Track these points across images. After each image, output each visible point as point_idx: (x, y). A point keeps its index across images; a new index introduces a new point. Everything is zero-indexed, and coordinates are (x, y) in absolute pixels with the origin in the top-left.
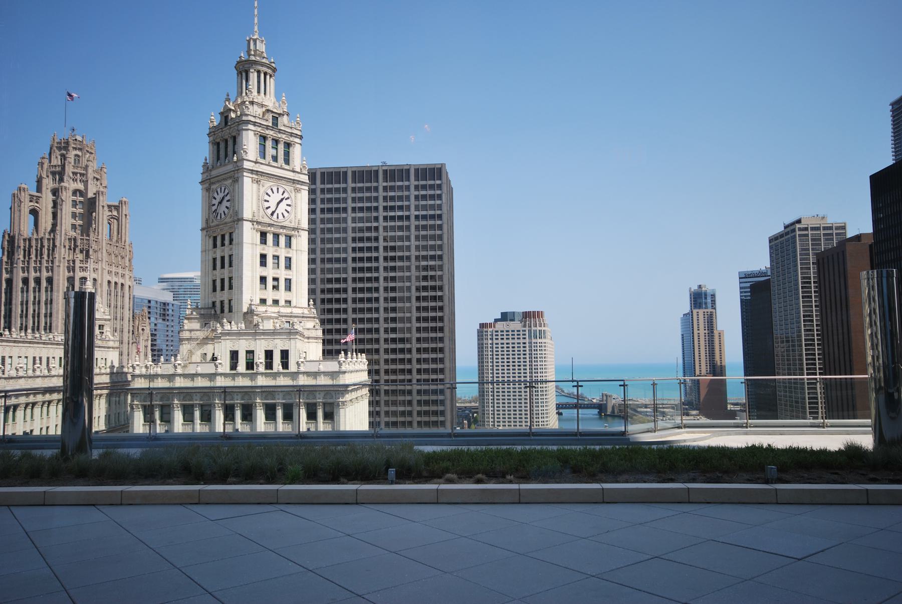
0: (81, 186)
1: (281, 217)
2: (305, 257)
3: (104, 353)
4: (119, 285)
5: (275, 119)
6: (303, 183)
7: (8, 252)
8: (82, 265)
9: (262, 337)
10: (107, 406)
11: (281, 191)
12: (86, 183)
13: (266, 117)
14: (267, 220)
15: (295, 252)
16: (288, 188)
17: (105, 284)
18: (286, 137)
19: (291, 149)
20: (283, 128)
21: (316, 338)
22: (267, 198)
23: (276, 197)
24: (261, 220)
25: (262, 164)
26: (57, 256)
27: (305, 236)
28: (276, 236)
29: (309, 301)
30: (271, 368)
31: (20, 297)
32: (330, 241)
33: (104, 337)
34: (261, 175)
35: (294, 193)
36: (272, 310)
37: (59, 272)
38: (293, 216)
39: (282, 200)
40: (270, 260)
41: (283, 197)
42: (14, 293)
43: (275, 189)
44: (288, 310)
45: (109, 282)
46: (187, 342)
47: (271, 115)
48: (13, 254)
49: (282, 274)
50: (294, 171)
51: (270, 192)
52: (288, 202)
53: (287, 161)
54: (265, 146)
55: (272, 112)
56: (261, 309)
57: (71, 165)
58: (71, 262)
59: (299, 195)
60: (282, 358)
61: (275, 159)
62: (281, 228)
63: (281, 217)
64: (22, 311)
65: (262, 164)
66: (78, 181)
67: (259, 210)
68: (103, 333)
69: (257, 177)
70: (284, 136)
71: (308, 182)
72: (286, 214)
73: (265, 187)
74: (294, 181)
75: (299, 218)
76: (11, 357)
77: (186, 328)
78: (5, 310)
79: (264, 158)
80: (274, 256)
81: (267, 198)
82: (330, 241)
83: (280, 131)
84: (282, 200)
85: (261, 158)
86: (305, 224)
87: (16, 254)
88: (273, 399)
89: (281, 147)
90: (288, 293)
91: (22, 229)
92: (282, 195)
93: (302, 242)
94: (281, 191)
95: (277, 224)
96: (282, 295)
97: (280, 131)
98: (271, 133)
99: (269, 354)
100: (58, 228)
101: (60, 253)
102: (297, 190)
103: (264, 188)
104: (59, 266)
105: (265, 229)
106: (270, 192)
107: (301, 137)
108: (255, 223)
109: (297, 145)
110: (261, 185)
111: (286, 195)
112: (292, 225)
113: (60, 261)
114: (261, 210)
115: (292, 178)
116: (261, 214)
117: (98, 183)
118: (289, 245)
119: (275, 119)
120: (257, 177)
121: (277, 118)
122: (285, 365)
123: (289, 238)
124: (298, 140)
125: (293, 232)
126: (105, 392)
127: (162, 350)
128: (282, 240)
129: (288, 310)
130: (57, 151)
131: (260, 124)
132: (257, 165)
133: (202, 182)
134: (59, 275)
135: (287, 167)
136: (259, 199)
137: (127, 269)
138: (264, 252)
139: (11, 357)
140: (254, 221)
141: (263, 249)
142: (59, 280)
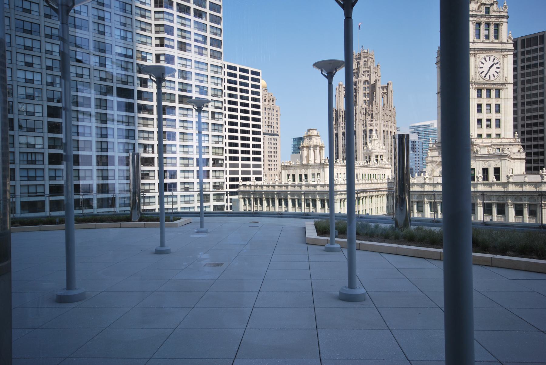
0: (367, 78)
1: (492, 77)
2: (511, 102)
3: (374, 171)
4: (386, 132)
5: (487, 9)
6: (509, 50)
7: (336, 119)
8: (370, 123)
9: (480, 159)
10: (387, 200)
11: (492, 58)
12: (370, 76)
13: (480, 9)
14: (482, 81)
15: (503, 100)
16: (497, 56)
17: (382, 132)
18: (496, 20)
19: (500, 27)
20: (493, 14)
21: (521, 159)
22: (481, 65)
23: (489, 63)
24: (477, 81)
25: (477, 43)
26: (357, 119)
27: (511, 88)
28: (489, 91)
29: (514, 133)
30: (487, 180)
31: (342, 143)
32: (529, 89)
33: (383, 162)
34: (477, 51)
35: (502, 58)
36: (487, 141)
37: (359, 128)
38: (501, 75)
39: (493, 65)
40: (484, 108)
41: (493, 63)
42: (339, 141)
43: (487, 59)
44: (498, 141)
45: (384, 131)
46: (430, 164)
47: (484, 6)
48: (338, 120)
49: (494, 116)
50: (502, 43)
51: (484, 61)
52: (498, 65)
53: (496, 37)
54: (479, 30)
55: (485, 4)
56: (479, 141)
57: (362, 67)
58: (364, 121)
59: (506, 59)
60: (495, 173)
61: (487, 37)
62: (492, 85)
63: (492, 77)
64: (343, 150)
65: (477, 43)
66: (366, 75)
67: (476, 75)
68: (382, 160)
69: (474, 53)
70: (494, 19)
71: (513, 48)
72: (496, 74)
73: (480, 58)
74: (502, 50)
75: (506, 75)
76: (341, 174)
77: (429, 155)
78: (336, 149)
79: (479, 38)
80: (487, 105)
81: (481, 65)
82: (529, 89)
83: (491, 17)
84: (493, 65)
85: (477, 39)
86: (511, 79)
87: (339, 120)
88: (489, 200)
89: (492, 28)
90: (498, 129)
91: (341, 106)
92: (493, 61)
93: (508, 93)
94: (492, 58)
95: (489, 82)
96: (494, 131)
97: (491, 17)
98: (484, 19)
99: (485, 171)
100: (357, 103)
101: (359, 117)
102: (504, 56)
103: (479, 59)
104: (359, 124)
105: (480, 87)
106: (484, 61)
107: (507, 17)
108: (473, 84)
109: (504, 23)
110: (477, 58)
111: (496, 61)
112: (501, 81)
113: (359, 122)
114: (478, 74)
115: (501, 48)
116: (477, 78)
117: (376, 75)
118: (498, 95)
119: (487, 9)
120: (474, 53)
121: (489, 7)
122: (498, 178)
123: (498, 91)
124: (505, 20)
125: (501, 87)
126: (386, 193)
127: (413, 169)
128: (493, 93)
129: (498, 141)
130: (355, 61)
131: (476, 15)
132: (474, 44)
133: (437, 63)
134: (359, 129)
135: (496, 41)
136: (476, 67)
137: (393, 122)
138: (480, 103)
139: (341, 174)
140: (473, 83)
141: (480, 101)
142: (359, 132)
